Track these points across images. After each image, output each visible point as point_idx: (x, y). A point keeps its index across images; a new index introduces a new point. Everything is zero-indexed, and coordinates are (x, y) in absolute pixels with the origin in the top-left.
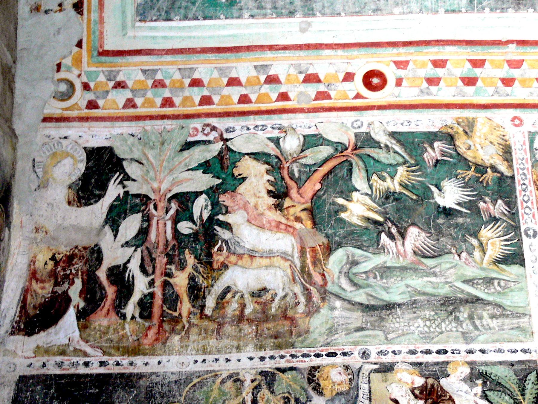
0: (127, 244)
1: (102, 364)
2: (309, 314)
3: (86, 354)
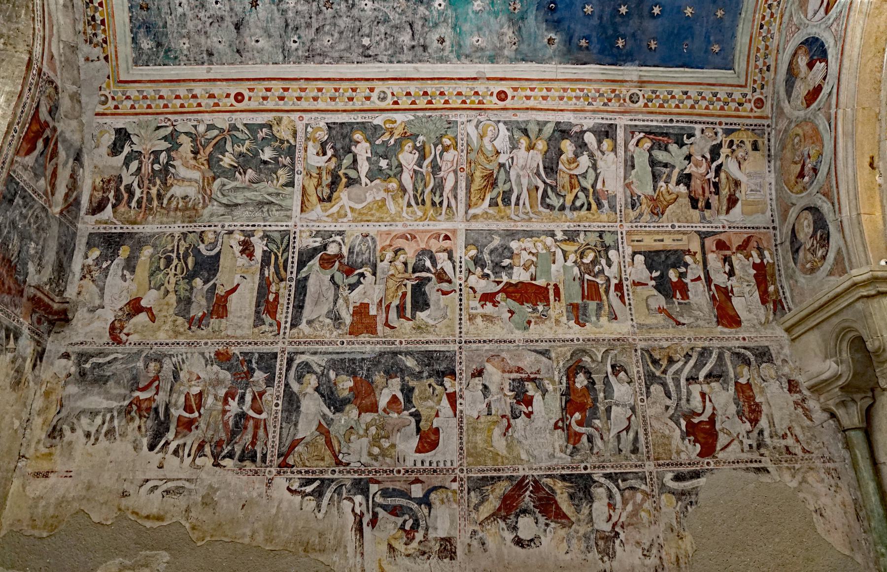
0: (132, 174)
1: (121, 228)
2: (203, 208)
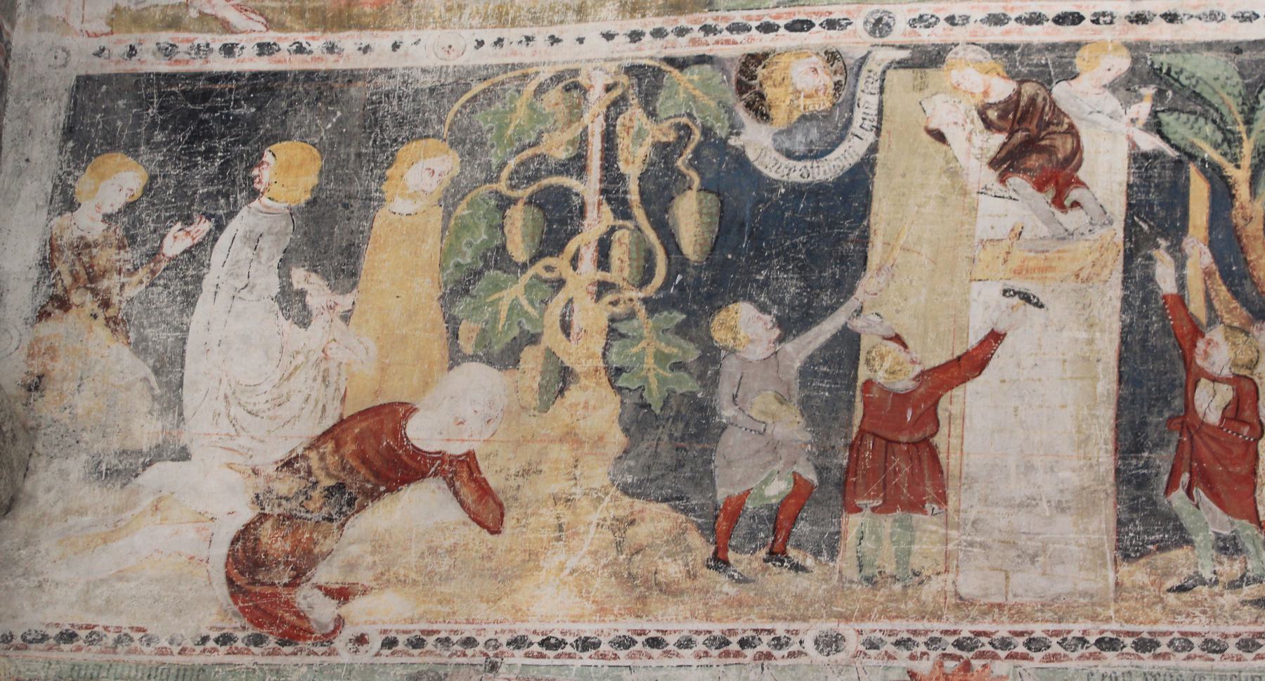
1: (265, 49)
3: (227, 27)
